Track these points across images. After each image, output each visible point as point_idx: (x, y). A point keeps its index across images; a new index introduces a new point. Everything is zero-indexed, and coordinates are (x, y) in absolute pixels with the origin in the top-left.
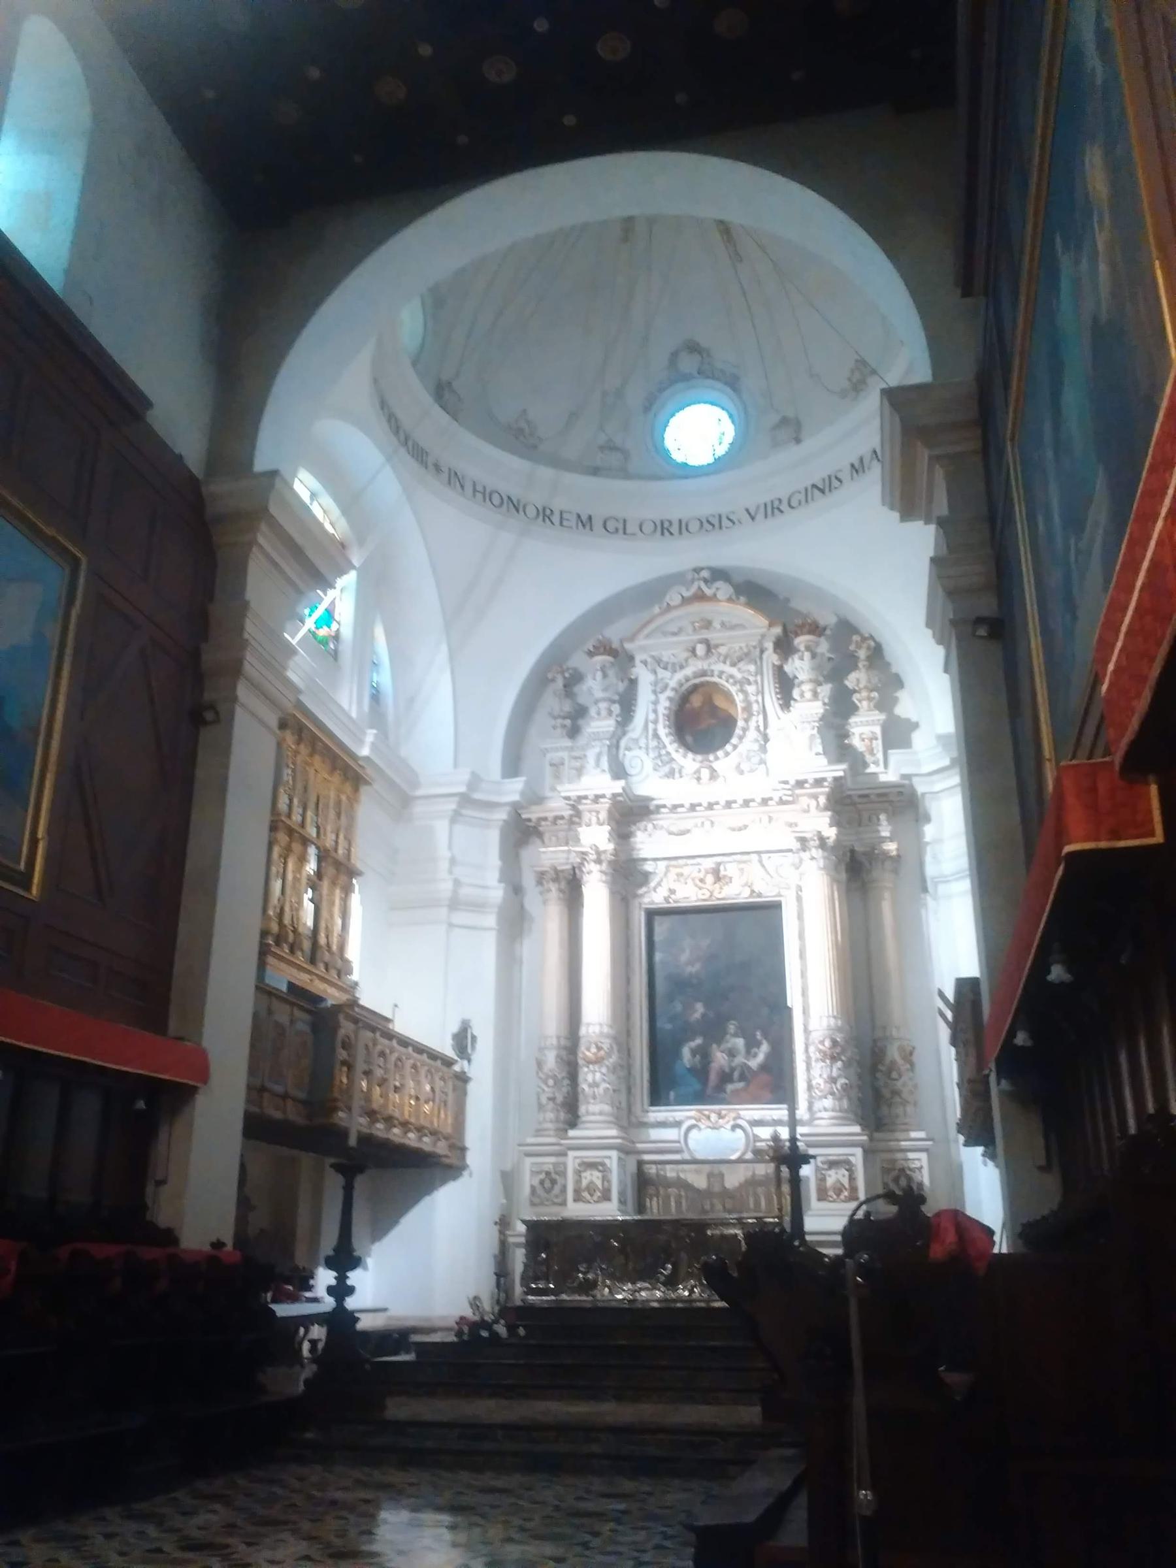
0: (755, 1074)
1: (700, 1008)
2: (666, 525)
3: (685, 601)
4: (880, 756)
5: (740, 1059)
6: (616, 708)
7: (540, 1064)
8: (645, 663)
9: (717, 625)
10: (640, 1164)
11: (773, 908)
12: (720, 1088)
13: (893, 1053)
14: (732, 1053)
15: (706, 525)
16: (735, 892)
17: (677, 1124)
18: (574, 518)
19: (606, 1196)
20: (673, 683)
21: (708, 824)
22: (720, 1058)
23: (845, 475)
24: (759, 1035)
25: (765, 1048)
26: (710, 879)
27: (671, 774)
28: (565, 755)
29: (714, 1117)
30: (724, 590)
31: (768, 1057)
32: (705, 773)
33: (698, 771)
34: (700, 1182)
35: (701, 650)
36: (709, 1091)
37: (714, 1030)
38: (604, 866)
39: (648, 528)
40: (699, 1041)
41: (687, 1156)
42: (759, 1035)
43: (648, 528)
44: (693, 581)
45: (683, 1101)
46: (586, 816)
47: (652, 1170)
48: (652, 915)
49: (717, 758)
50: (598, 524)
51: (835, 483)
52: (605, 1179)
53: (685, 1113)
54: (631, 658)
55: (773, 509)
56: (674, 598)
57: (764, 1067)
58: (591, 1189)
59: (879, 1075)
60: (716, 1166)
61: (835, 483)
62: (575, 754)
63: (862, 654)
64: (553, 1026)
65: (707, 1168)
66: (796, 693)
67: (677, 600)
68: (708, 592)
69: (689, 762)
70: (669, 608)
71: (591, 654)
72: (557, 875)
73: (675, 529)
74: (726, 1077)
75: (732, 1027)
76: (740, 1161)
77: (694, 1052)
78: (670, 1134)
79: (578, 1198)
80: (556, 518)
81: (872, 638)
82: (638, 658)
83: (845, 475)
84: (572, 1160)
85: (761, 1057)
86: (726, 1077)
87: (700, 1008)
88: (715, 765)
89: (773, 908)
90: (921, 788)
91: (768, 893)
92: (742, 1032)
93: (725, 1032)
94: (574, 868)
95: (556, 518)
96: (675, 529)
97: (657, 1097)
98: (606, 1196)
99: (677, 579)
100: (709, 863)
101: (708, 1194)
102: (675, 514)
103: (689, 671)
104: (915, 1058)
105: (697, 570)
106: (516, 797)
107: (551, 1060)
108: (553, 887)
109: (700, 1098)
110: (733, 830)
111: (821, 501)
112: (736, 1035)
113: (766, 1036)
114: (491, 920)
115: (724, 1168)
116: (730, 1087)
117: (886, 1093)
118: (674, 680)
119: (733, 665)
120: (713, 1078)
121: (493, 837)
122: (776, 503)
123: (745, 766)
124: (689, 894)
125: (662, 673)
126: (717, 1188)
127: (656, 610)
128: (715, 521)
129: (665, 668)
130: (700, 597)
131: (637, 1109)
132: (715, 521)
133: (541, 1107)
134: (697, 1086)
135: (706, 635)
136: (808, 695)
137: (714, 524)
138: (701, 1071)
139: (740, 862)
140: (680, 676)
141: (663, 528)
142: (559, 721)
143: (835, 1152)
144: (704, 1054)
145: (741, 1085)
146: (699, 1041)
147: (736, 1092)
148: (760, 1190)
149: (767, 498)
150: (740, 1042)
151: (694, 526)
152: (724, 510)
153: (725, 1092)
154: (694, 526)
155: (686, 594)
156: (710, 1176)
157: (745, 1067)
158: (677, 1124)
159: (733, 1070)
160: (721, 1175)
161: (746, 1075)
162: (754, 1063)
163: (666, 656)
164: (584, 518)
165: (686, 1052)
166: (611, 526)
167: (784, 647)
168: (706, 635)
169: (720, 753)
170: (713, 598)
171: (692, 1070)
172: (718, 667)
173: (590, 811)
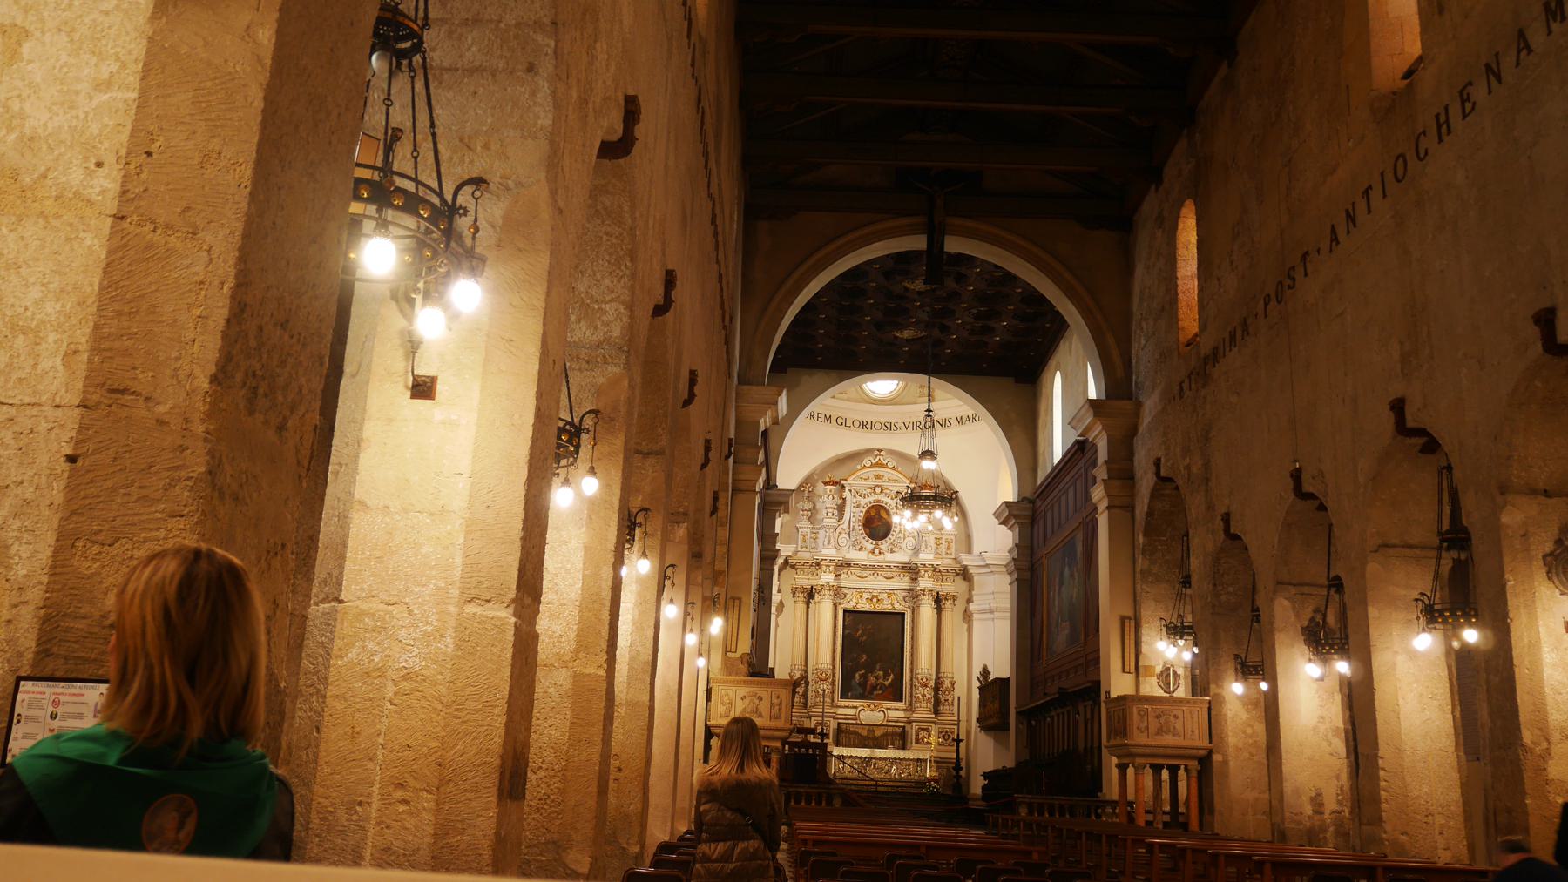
0: (886, 688)
1: (864, 657)
2: (865, 423)
3: (872, 465)
4: (953, 550)
5: (881, 681)
6: (836, 512)
8: (850, 491)
9: (885, 478)
10: (839, 723)
12: (871, 692)
13: (947, 683)
14: (877, 678)
15: (884, 426)
16: (885, 606)
17: (856, 707)
18: (823, 416)
20: (862, 504)
21: (876, 574)
22: (872, 679)
23: (953, 421)
24: (890, 671)
26: (875, 600)
27: (861, 549)
28: (809, 531)
29: (872, 706)
32: (877, 551)
33: (873, 549)
34: (864, 732)
35: (878, 490)
36: (866, 694)
37: (870, 669)
38: (832, 593)
39: (857, 424)
40: (863, 672)
41: (859, 722)
42: (890, 671)
43: (857, 424)
44: (877, 456)
46: (824, 568)
49: (882, 544)
51: (948, 424)
54: (843, 487)
56: (867, 461)
59: (940, 693)
61: (948, 424)
62: (814, 531)
65: (867, 727)
67: (869, 464)
68: (885, 462)
69: (869, 545)
71: (825, 484)
72: (803, 590)
73: (868, 426)
74: (874, 688)
75: (878, 667)
76: (880, 725)
77: (861, 676)
78: (852, 711)
80: (815, 417)
82: (847, 489)
83: (953, 421)
85: (890, 680)
86: (874, 688)
87: (864, 657)
88: (882, 547)
89: (903, 614)
90: (971, 571)
91: (899, 608)
94: (812, 587)
95: (815, 417)
97: (844, 695)
99: (868, 452)
100: (875, 593)
103: (873, 498)
104: (955, 686)
105: (880, 451)
106: (790, 554)
108: (801, 595)
110: (887, 578)
112: (880, 670)
113: (892, 672)
115: (875, 728)
116: (875, 693)
117: (943, 700)
118: (863, 501)
119: (892, 499)
120: (868, 687)
122: (918, 424)
123: (896, 550)
124: (864, 606)
126: (871, 736)
127: (859, 467)
128: (889, 426)
129: (860, 496)
130: (879, 464)
131: (836, 700)
132: (889, 426)
134: (861, 691)
135: (879, 482)
137: (888, 427)
138: (863, 685)
139: (889, 593)
140: (867, 500)
141: (864, 425)
142: (805, 512)
143: (924, 725)
145: (880, 692)
147: (878, 695)
148: (890, 738)
150: (881, 673)
151: (878, 426)
152: (893, 421)
153: (872, 694)
154: (878, 426)
155: (874, 462)
156: (868, 730)
158: (856, 707)
159: (877, 685)
160: (874, 731)
161: (882, 687)
162: (886, 683)
163: (862, 490)
164: (828, 417)
165: (857, 675)
166: (840, 421)
168: (879, 482)
169: (883, 541)
170: (886, 466)
171: (859, 684)
172: (885, 499)
173: (826, 566)
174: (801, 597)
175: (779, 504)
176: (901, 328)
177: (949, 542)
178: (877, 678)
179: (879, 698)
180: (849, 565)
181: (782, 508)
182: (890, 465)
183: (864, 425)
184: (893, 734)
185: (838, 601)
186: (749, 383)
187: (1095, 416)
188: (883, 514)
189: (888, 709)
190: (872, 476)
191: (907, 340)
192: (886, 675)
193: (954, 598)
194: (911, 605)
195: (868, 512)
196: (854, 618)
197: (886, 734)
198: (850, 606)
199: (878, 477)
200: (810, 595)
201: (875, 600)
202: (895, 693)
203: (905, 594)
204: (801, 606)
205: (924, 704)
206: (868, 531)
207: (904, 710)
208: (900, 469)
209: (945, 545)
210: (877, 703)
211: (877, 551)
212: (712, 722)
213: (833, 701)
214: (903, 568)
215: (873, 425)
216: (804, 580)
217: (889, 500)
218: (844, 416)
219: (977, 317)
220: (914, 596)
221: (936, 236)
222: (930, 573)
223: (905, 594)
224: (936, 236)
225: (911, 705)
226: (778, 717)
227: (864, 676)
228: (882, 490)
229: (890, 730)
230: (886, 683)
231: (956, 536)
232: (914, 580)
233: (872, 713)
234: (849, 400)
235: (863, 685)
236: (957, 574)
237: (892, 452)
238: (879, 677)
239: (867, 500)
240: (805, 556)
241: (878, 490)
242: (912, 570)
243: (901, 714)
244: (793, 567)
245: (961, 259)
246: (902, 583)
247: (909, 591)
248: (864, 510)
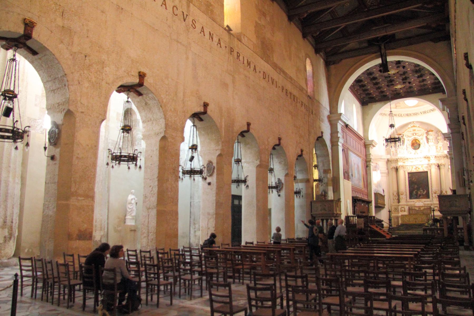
0: (424, 195)
3: (412, 127)
5: (422, 193)
7: (393, 194)
9: (417, 130)
10: (409, 207)
11: (427, 172)
16: (421, 170)
19: (405, 211)
22: (419, 193)
25: (426, 191)
30: (417, 125)
31: (426, 192)
34: (417, 209)
35: (414, 134)
37: (418, 189)
39: (405, 115)
40: (416, 190)
45: (414, 198)
46: (399, 161)
47: (410, 208)
48: (408, 173)
50: (397, 115)
52: (405, 209)
53: (415, 200)
55: (425, 112)
56: (409, 126)
57: (425, 194)
58: (403, 210)
60: (419, 207)
63: (439, 134)
64: (395, 189)
66: (429, 141)
67: (410, 127)
70: (409, 128)
72: (394, 168)
73: (409, 115)
74: (420, 195)
75: (421, 188)
76: (423, 206)
77: (415, 192)
78: (412, 203)
79: (401, 211)
81: (441, 131)
82: (405, 135)
84: (400, 207)
86: (420, 195)
89: (427, 172)
91: (426, 170)
92: (422, 189)
93: (420, 189)
96: (409, 115)
98: (405, 211)
99: (410, 123)
100: (417, 166)
101: (418, 211)
102: (409, 113)
105: (413, 122)
107: (395, 194)
108: (394, 170)
109: (416, 198)
111: (432, 113)
114: (385, 175)
116: (421, 197)
120: (418, 195)
121: (385, 163)
125: (408, 138)
127: (407, 128)
130: (414, 126)
131: (408, 200)
133: (394, 200)
134: (416, 196)
136: (431, 141)
137: (415, 114)
138: (416, 195)
140: (411, 138)
141: (407, 115)
144: (417, 192)
146: (416, 190)
149: (423, 110)
150: (422, 191)
152: (417, 112)
157: (423, 194)
161: (423, 195)
162: (424, 193)
163: (409, 135)
165: (414, 192)
166: (399, 115)
167: (427, 133)
170: (416, 127)
171: (415, 195)
174: (394, 171)
175: (370, 145)
176: (397, 85)
177: (440, 147)
178: (421, 192)
179: (422, 198)
180: (407, 159)
181: (371, 146)
182: (417, 126)
183: (407, 115)
184: (427, 209)
185: (405, 170)
186: (333, 113)
187: (443, 104)
188: (417, 141)
189: (424, 201)
190: (412, 130)
191: (400, 88)
192: (424, 191)
193: (444, 165)
194: (429, 168)
195: (412, 141)
196: (411, 175)
197: (425, 209)
198: (409, 171)
199: (414, 130)
200: (397, 169)
201: (417, 168)
202: (427, 196)
203: (427, 165)
204: (394, 173)
205: (435, 199)
206: (413, 147)
207: (431, 201)
208: (421, 127)
209: (439, 148)
210: (420, 200)
211: (416, 153)
212: (312, 213)
213: (407, 200)
214: (425, 157)
215: (410, 115)
216: (394, 165)
217: (419, 137)
218: (400, 113)
219: (418, 77)
220: (430, 165)
221: (383, 57)
222: (434, 158)
223: (427, 165)
224: (383, 57)
225: (432, 199)
226: (330, 211)
227: (417, 192)
228: (416, 134)
229: (426, 207)
230: (424, 193)
231: (443, 145)
232: (429, 161)
233: (419, 203)
234: (401, 108)
235: (416, 195)
236: (444, 157)
237: (417, 122)
238: (421, 192)
239: (411, 138)
240: (394, 157)
241: (414, 134)
242: (427, 158)
243: (429, 203)
244: (391, 161)
245: (398, 62)
246: (426, 161)
247: (428, 164)
248: (411, 141)
